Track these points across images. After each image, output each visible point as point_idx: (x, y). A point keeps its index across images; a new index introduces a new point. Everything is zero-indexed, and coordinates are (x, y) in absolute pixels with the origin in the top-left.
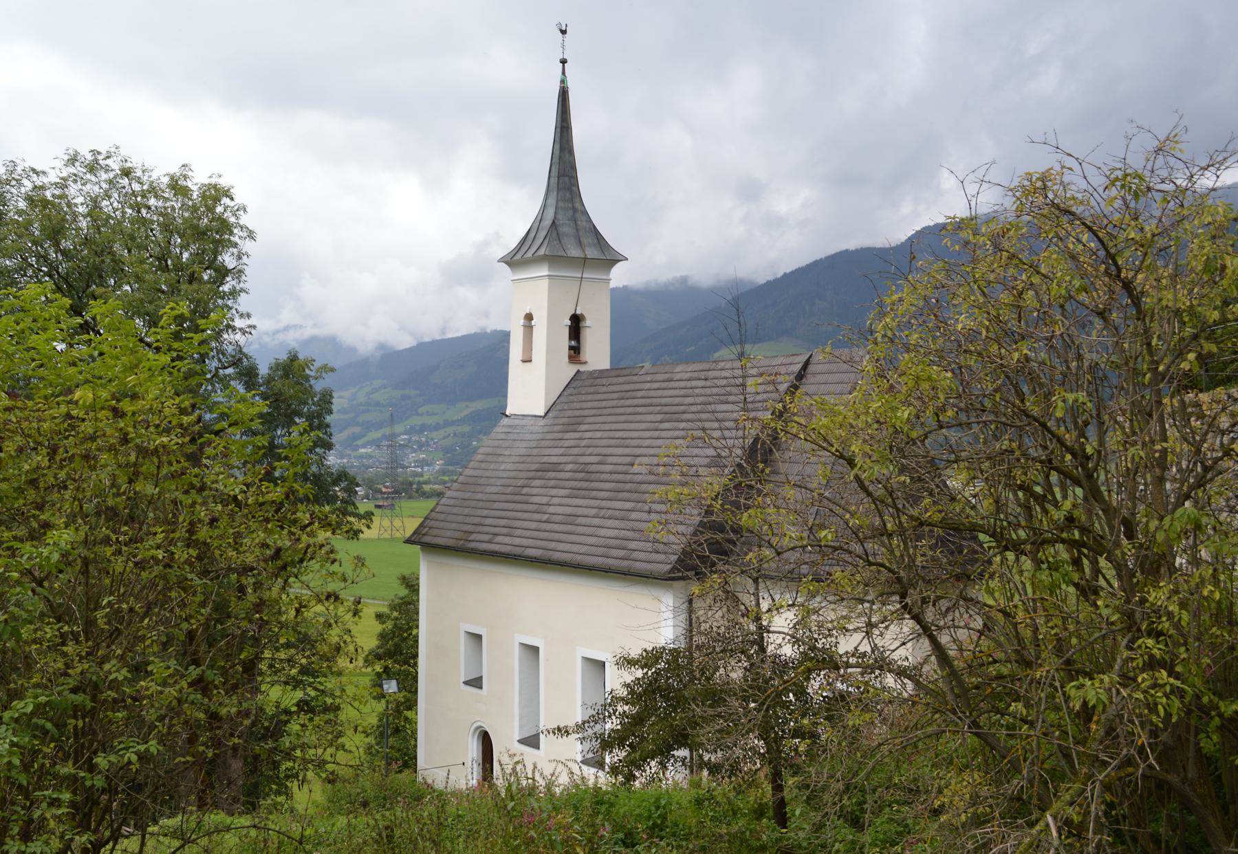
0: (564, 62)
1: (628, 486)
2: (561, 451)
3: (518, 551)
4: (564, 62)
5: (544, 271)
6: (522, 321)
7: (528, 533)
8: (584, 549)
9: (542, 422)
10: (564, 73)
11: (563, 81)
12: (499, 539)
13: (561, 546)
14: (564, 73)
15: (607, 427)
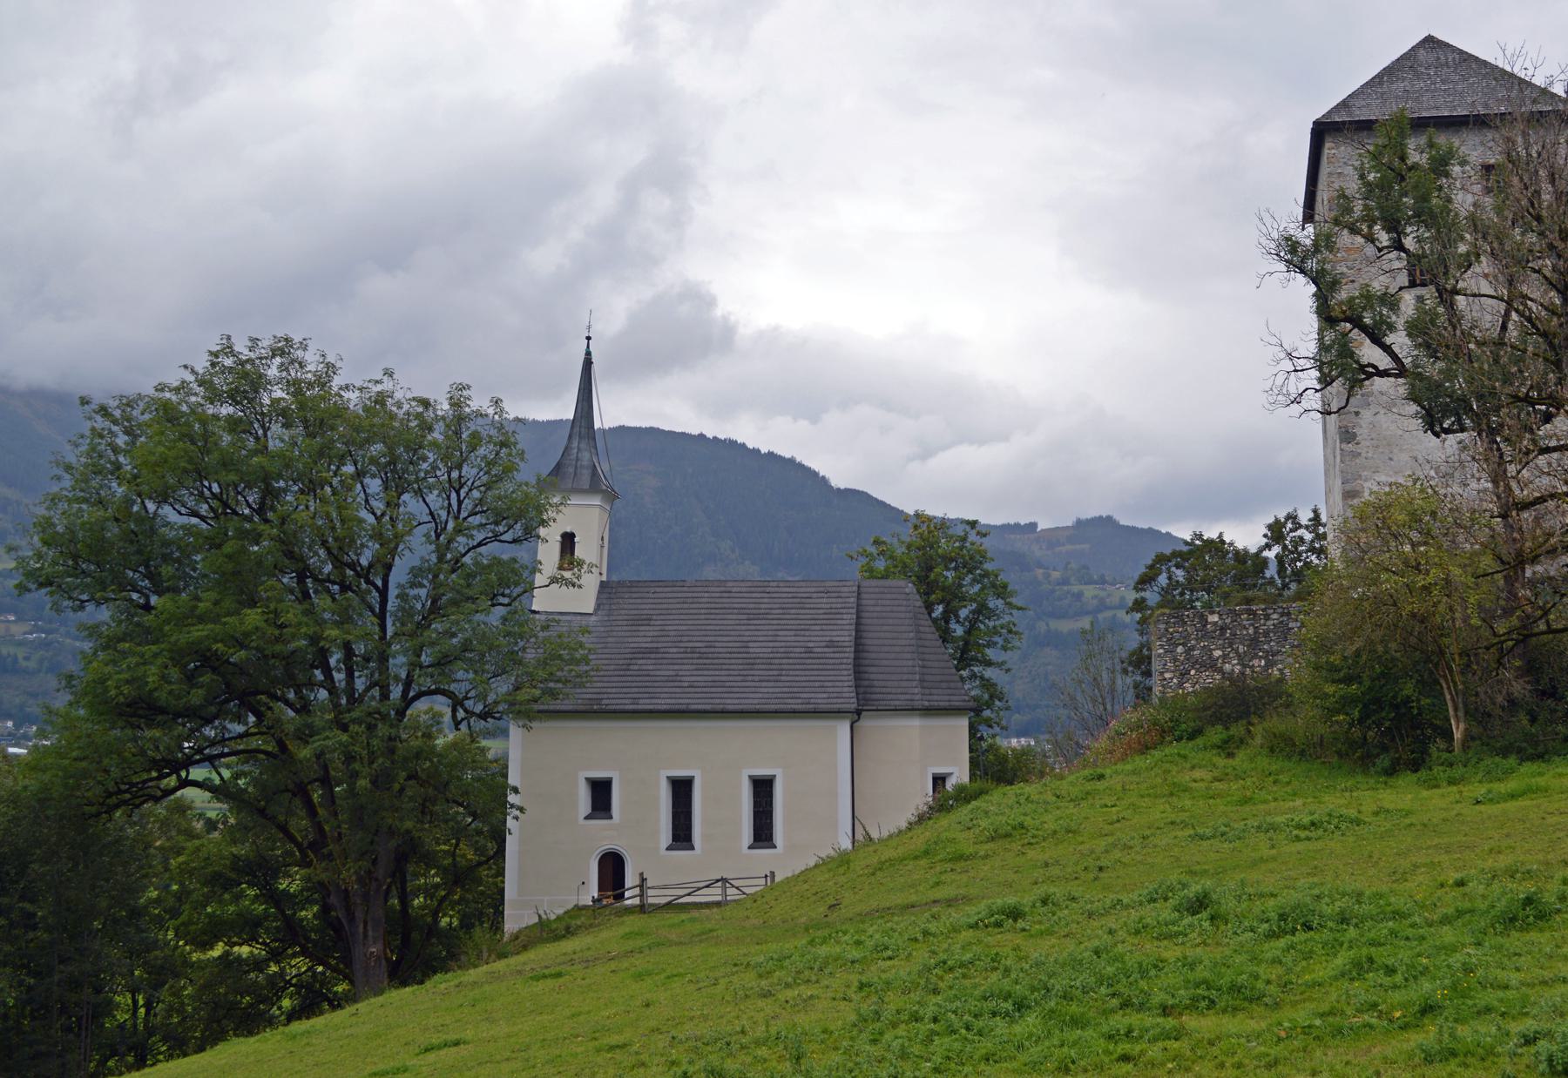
0: (589, 338)
1: (758, 661)
2: (649, 639)
3: (684, 707)
4: (589, 338)
5: (596, 501)
6: (559, 538)
7: (677, 696)
8: (756, 701)
9: (593, 618)
10: (588, 347)
11: (588, 353)
12: (641, 701)
13: (729, 701)
14: (588, 347)
15: (690, 622)
